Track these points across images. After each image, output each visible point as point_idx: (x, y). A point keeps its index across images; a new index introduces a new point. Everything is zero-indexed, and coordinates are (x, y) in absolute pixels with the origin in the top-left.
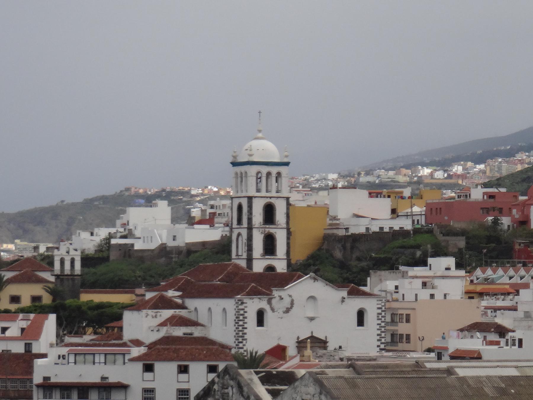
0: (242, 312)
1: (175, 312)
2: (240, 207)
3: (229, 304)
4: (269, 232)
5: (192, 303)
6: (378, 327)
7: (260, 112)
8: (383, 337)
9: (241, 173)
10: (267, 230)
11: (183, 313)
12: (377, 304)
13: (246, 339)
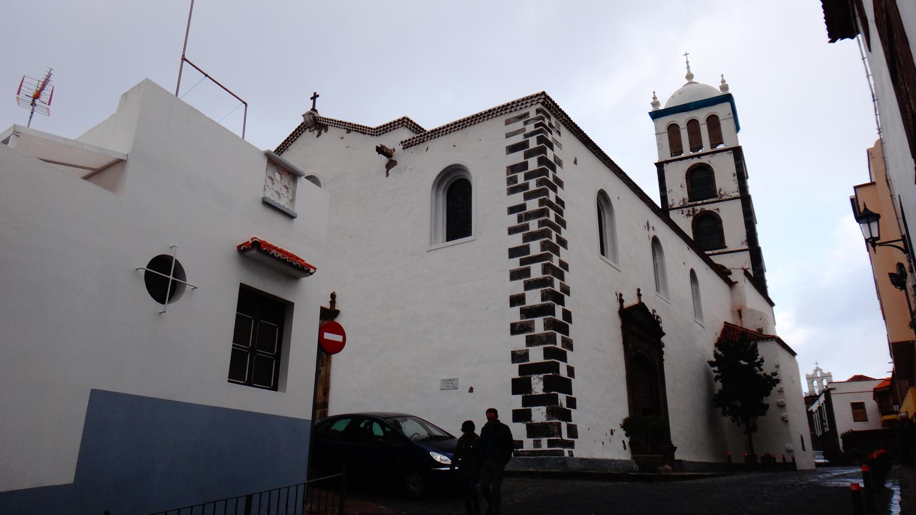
4: (703, 211)
8: (535, 259)
10: (698, 208)
12: (508, 136)
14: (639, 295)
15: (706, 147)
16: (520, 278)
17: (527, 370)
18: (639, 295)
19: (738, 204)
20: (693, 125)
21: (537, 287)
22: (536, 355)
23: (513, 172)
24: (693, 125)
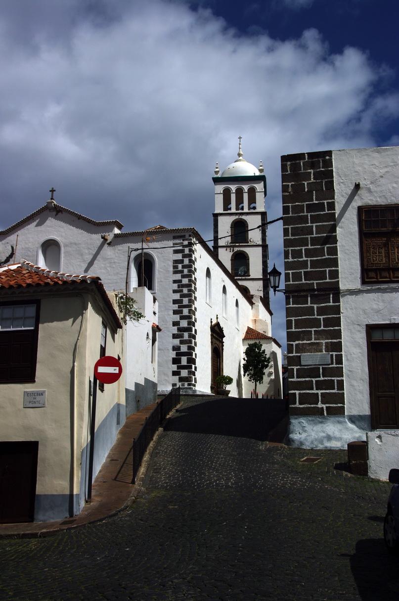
14: (217, 318)
15: (246, 210)
16: (178, 314)
17: (180, 354)
18: (217, 318)
20: (239, 192)
21: (186, 319)
22: (184, 348)
24: (239, 192)
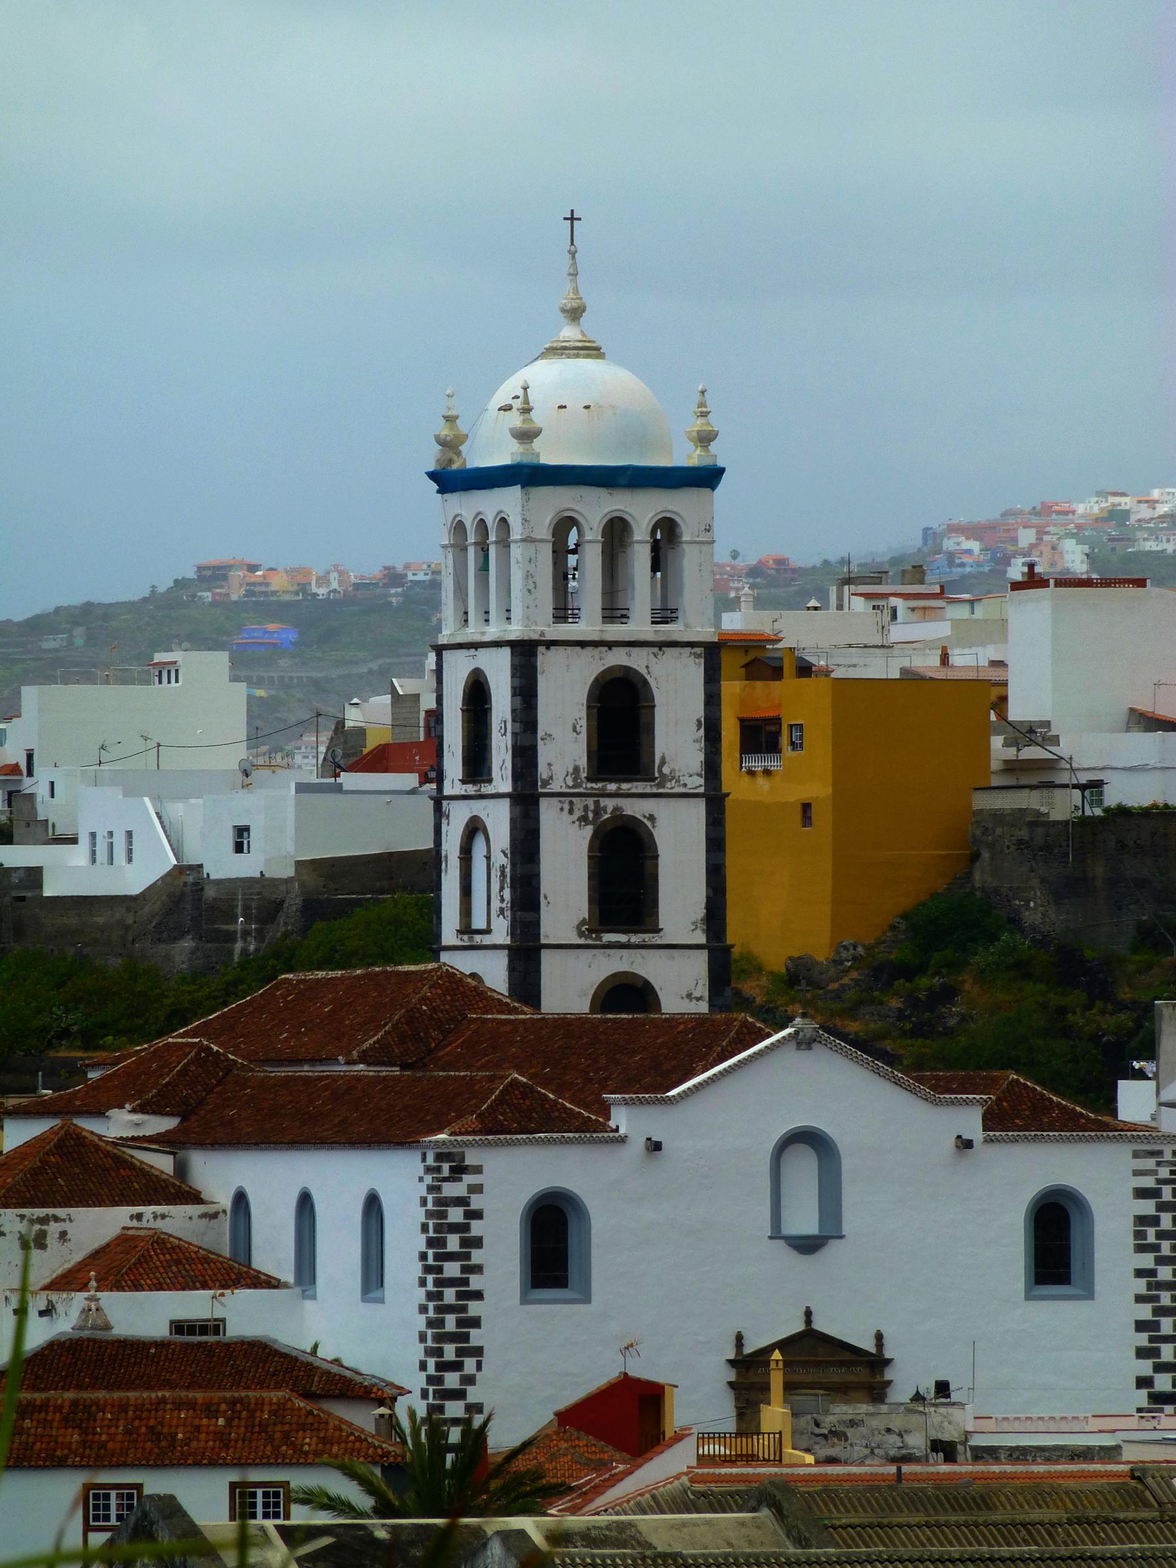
0: (455, 1215)
1: (139, 1217)
2: (477, 694)
3: (399, 1178)
4: (617, 812)
5: (219, 1174)
6: (1141, 1286)
7: (572, 219)
9: (482, 525)
10: (609, 804)
11: (176, 1221)
12: (1137, 1173)
13: (478, 1352)
19: (697, 812)
20: (616, 533)
21: (1168, 1372)
23: (1141, 1224)
24: (616, 533)
